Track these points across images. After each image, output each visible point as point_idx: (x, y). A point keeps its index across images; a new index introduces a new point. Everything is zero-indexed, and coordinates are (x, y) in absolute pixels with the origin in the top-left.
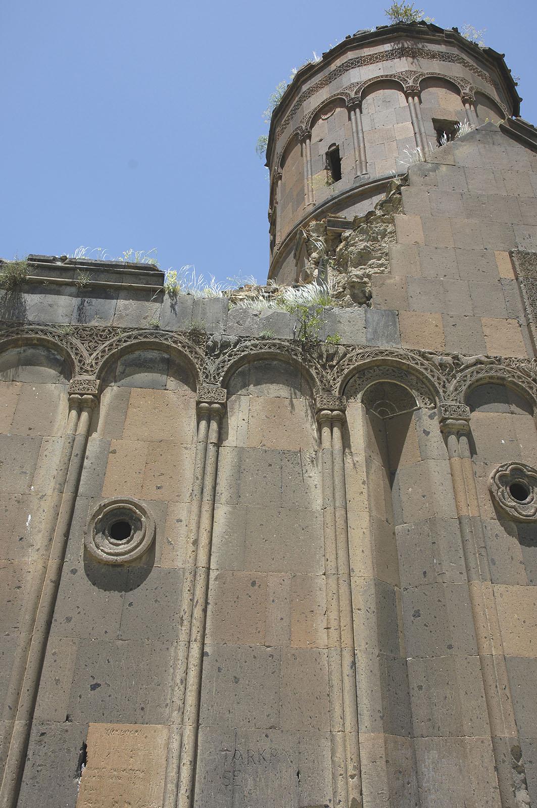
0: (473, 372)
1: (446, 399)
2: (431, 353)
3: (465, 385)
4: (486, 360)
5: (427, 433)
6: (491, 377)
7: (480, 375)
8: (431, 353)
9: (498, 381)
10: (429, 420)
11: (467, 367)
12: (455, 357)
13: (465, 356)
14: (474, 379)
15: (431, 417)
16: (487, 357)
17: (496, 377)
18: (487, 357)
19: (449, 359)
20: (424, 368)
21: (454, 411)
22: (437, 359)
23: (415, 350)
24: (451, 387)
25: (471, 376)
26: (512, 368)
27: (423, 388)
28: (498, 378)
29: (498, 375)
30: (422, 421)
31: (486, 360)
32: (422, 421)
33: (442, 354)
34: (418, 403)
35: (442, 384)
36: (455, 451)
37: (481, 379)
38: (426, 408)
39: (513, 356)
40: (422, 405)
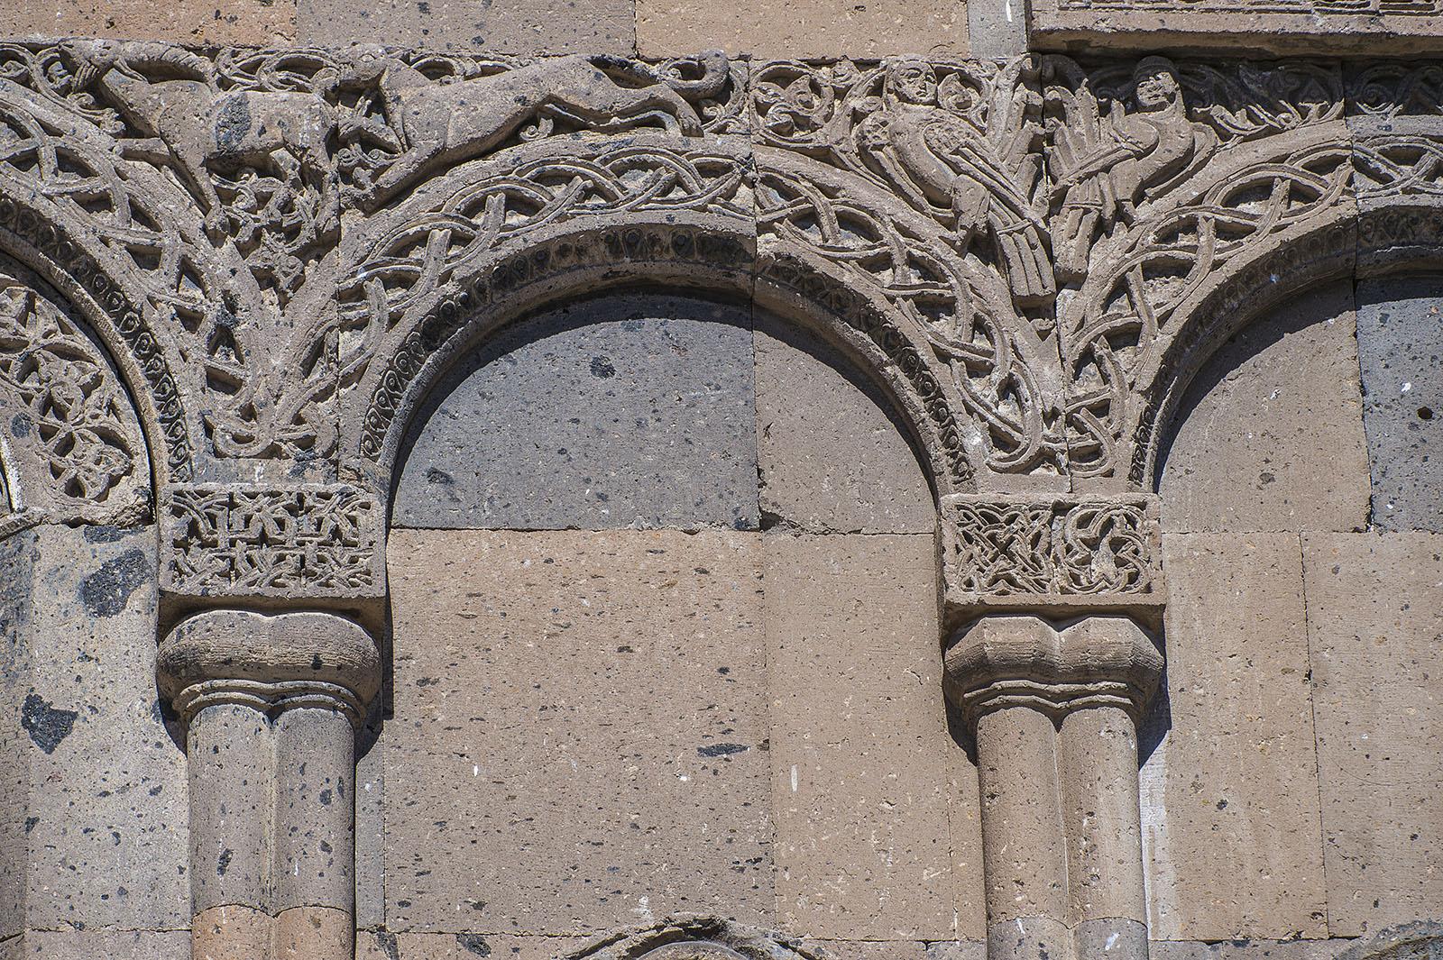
0: (477, 206)
1: (221, 441)
2: (157, 71)
3: (394, 320)
4: (606, 94)
5: (48, 724)
6: (627, 241)
7: (542, 231)
8: (157, 71)
9: (678, 269)
10: (80, 615)
11: (440, 163)
12: (362, 90)
13: (436, 70)
14: (478, 260)
15: (100, 595)
16: (619, 71)
17: (667, 240)
18: (619, 71)
19: (297, 115)
20: (76, 196)
21: (263, 539)
22: (194, 118)
23: (35, 48)
24: (273, 339)
25: (458, 239)
26: (825, 155)
27: (73, 355)
28: (687, 242)
29: (685, 217)
30: (25, 631)
31: (606, 94)
32: (25, 631)
33: (252, 69)
34: (14, 489)
35: (212, 312)
36: (225, 859)
37: (539, 258)
38: (74, 524)
39: (845, 40)
40: (49, 500)
